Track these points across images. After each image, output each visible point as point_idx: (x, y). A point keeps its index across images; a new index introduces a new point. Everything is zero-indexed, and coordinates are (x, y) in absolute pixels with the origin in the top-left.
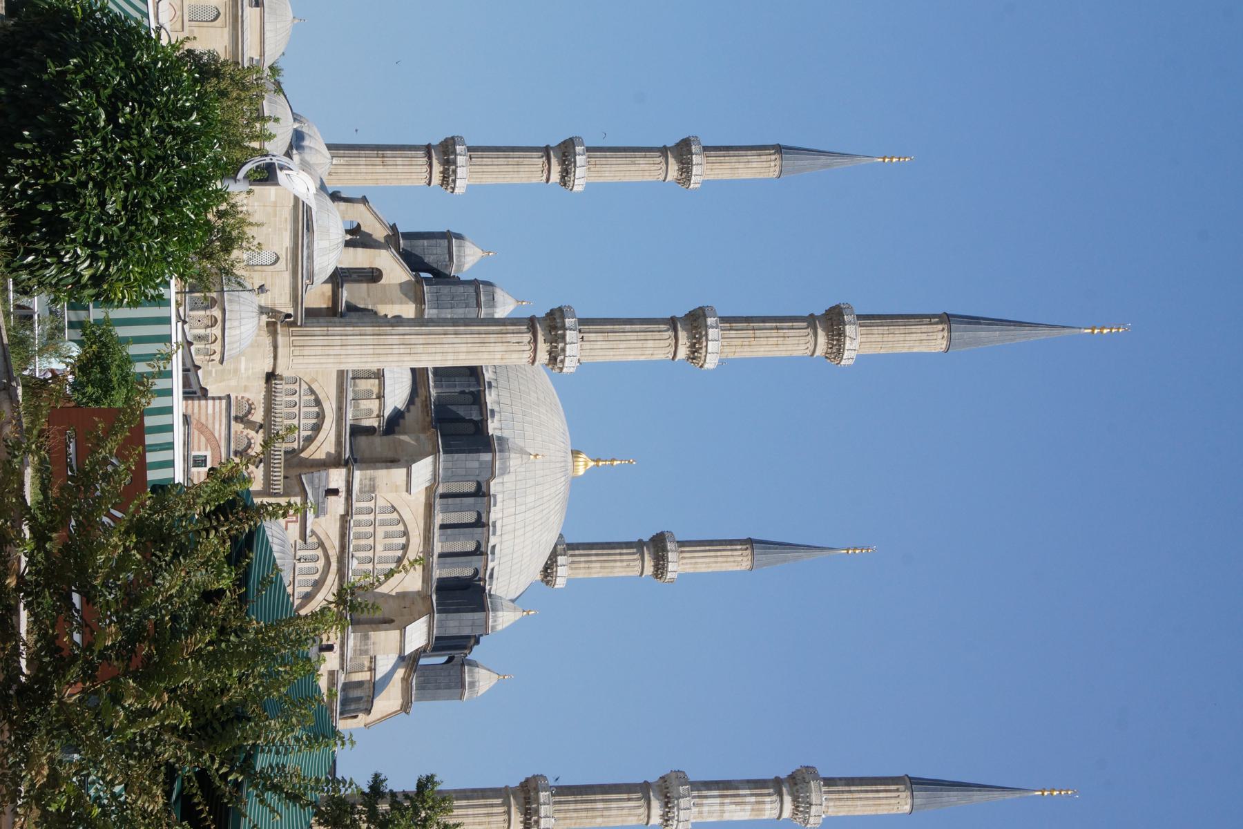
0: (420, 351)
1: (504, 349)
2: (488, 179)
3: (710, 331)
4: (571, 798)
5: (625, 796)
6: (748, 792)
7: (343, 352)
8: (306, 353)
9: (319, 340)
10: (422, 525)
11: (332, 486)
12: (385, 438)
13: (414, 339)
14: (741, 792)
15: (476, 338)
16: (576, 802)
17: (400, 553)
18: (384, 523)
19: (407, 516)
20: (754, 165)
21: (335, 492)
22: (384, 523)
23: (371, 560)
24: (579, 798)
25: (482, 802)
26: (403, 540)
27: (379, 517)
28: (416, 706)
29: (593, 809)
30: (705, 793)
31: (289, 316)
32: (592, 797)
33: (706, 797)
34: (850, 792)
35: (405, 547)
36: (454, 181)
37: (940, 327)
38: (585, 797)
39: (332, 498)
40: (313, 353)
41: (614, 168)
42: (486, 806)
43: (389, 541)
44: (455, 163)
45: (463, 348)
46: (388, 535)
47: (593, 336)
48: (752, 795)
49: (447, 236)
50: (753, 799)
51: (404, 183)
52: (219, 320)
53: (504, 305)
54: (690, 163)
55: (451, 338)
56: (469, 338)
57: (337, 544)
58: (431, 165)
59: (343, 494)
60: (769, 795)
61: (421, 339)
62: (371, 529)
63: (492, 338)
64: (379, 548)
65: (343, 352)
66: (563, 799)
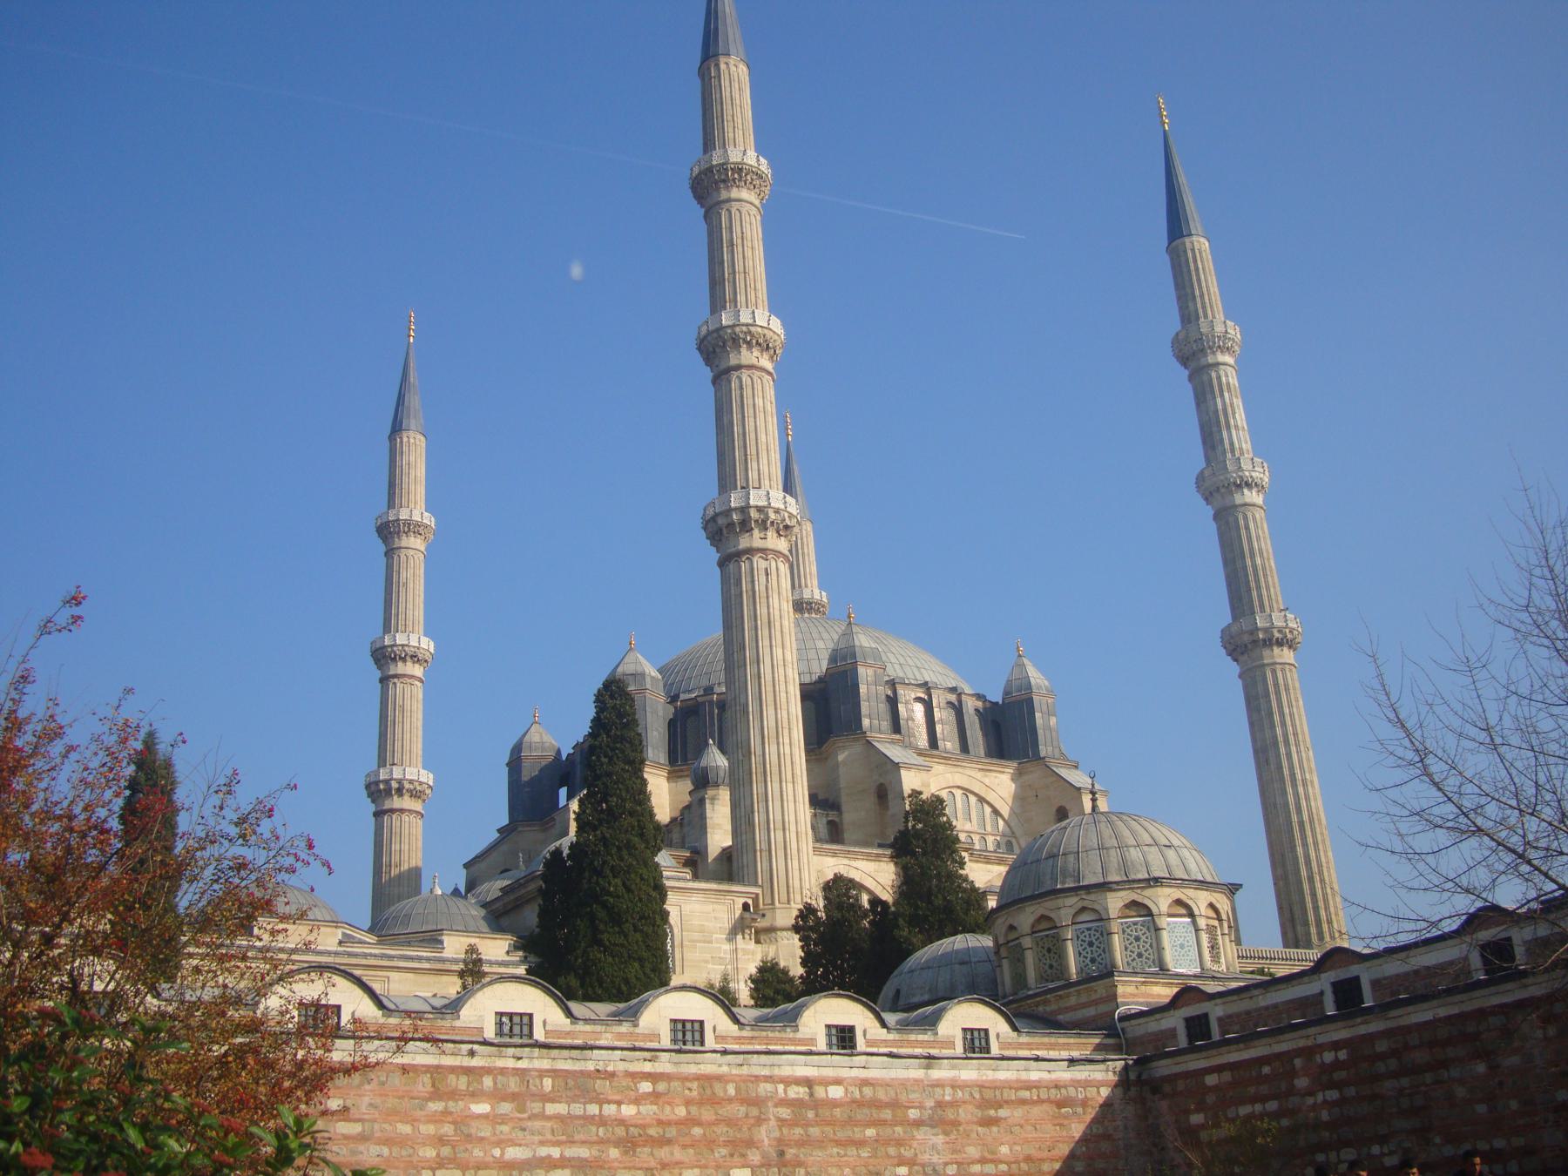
0: (785, 713)
1: (776, 596)
2: (418, 747)
3: (743, 320)
4: (1254, 594)
5: (1243, 532)
6: (1219, 400)
7: (793, 828)
8: (797, 884)
9: (778, 864)
12: (844, 808)
13: (770, 721)
14: (1220, 406)
15: (763, 633)
16: (1259, 588)
17: (973, 799)
20: (412, 459)
24: (1253, 584)
25: (1273, 697)
26: (958, 793)
29: (1264, 569)
30: (1227, 446)
31: (746, 907)
32: (1250, 571)
33: (1232, 444)
34: (1202, 296)
35: (967, 791)
36: (421, 783)
37: (723, 66)
38: (1251, 578)
40: (796, 873)
41: (410, 606)
42: (1278, 693)
44: (400, 782)
45: (778, 652)
47: (753, 475)
48: (1222, 396)
49: (515, 764)
50: (1226, 395)
51: (420, 844)
52: (1177, 894)
53: (637, 662)
54: (408, 523)
55: (766, 668)
56: (764, 643)
58: (402, 811)
60: (1219, 378)
61: (769, 713)
63: (762, 611)
65: (793, 828)
66: (1256, 603)
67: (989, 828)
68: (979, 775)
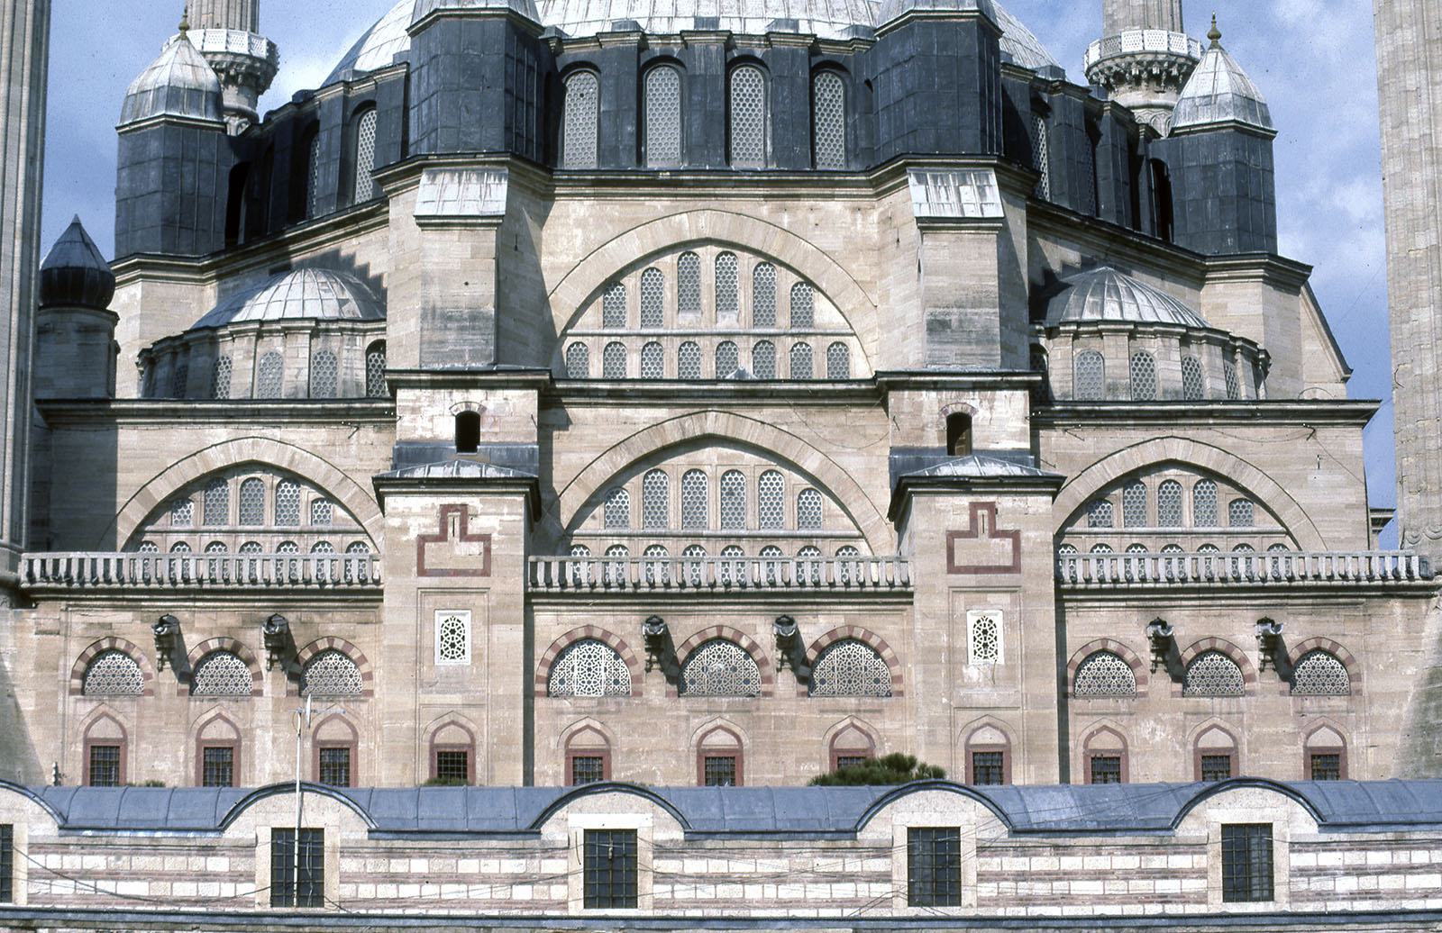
10: (661, 205)
11: (447, 430)
17: (746, 262)
18: (651, 311)
19: (633, 248)
21: (468, 427)
22: (651, 311)
23: (764, 344)
27: (632, 322)
28: (1288, 247)
35: (729, 246)
39: (487, 433)
43: (707, 299)
46: (688, 300)
57: (645, 415)
59: (476, 397)
62: (671, 348)
64: (727, 322)
67: (783, 321)
68: (765, 209)
